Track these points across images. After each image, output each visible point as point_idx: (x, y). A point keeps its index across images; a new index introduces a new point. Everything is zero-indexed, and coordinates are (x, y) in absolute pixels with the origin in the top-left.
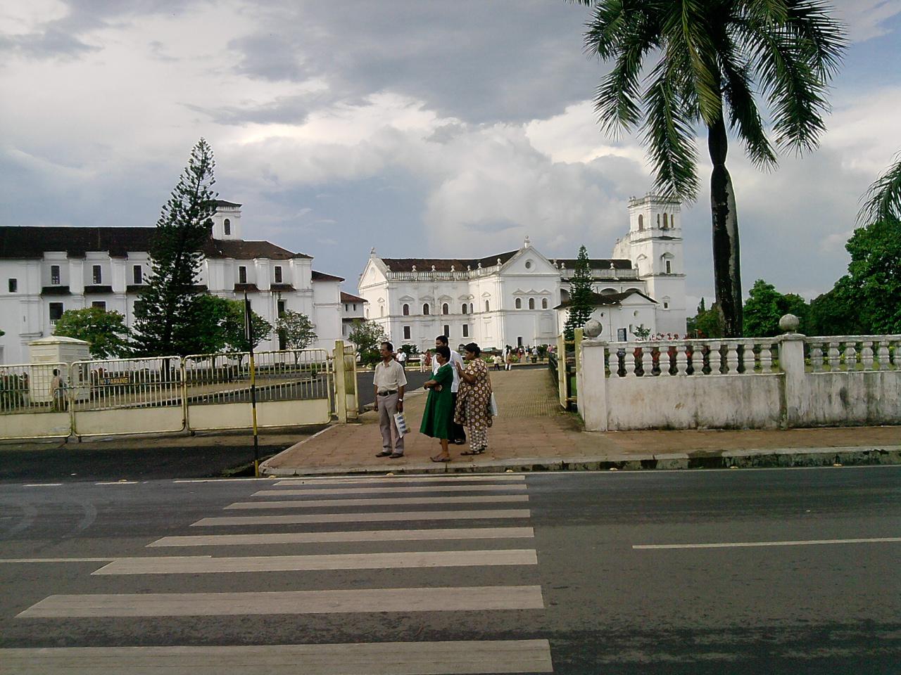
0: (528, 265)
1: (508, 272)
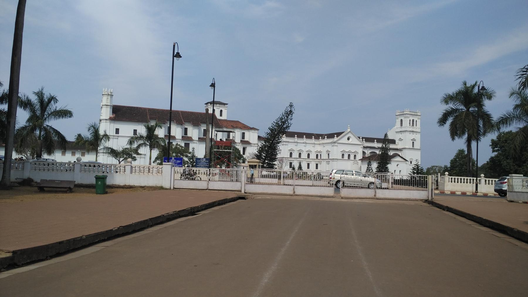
0: (348, 139)
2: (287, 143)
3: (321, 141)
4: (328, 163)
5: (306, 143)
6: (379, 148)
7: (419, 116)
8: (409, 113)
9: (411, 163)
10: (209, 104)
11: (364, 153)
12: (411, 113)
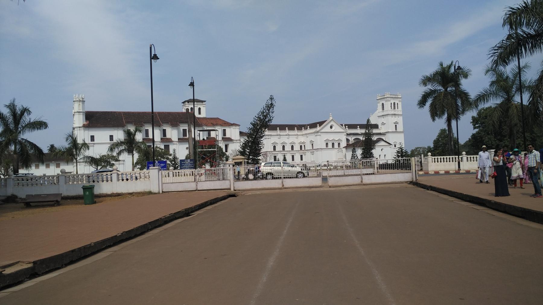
0: (331, 127)
1: (322, 131)
2: (269, 137)
3: (304, 132)
4: (313, 153)
5: (289, 135)
6: (362, 134)
7: (400, 98)
8: (389, 96)
9: (395, 146)
10: (187, 103)
11: (348, 140)
12: (392, 96)
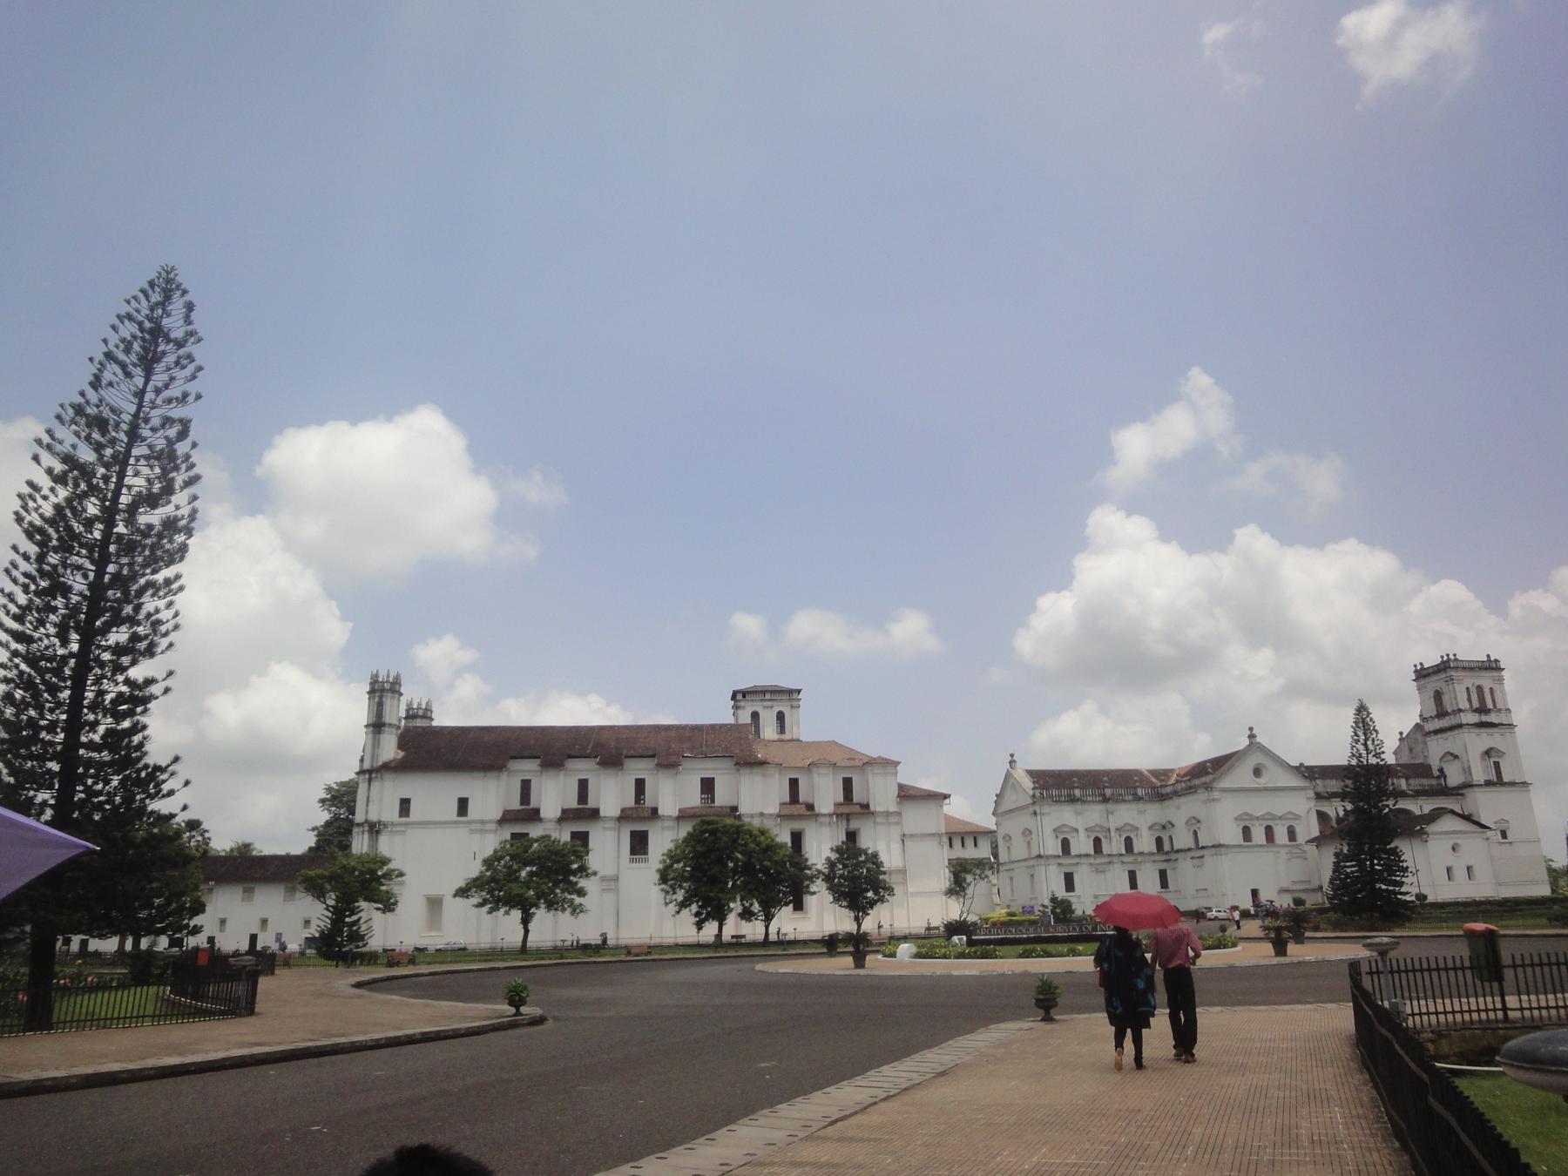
0: (1257, 772)
11: (1322, 816)
